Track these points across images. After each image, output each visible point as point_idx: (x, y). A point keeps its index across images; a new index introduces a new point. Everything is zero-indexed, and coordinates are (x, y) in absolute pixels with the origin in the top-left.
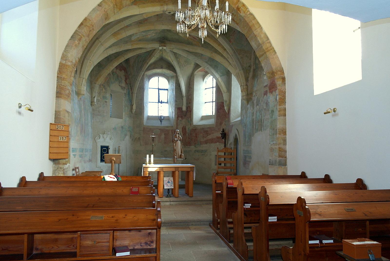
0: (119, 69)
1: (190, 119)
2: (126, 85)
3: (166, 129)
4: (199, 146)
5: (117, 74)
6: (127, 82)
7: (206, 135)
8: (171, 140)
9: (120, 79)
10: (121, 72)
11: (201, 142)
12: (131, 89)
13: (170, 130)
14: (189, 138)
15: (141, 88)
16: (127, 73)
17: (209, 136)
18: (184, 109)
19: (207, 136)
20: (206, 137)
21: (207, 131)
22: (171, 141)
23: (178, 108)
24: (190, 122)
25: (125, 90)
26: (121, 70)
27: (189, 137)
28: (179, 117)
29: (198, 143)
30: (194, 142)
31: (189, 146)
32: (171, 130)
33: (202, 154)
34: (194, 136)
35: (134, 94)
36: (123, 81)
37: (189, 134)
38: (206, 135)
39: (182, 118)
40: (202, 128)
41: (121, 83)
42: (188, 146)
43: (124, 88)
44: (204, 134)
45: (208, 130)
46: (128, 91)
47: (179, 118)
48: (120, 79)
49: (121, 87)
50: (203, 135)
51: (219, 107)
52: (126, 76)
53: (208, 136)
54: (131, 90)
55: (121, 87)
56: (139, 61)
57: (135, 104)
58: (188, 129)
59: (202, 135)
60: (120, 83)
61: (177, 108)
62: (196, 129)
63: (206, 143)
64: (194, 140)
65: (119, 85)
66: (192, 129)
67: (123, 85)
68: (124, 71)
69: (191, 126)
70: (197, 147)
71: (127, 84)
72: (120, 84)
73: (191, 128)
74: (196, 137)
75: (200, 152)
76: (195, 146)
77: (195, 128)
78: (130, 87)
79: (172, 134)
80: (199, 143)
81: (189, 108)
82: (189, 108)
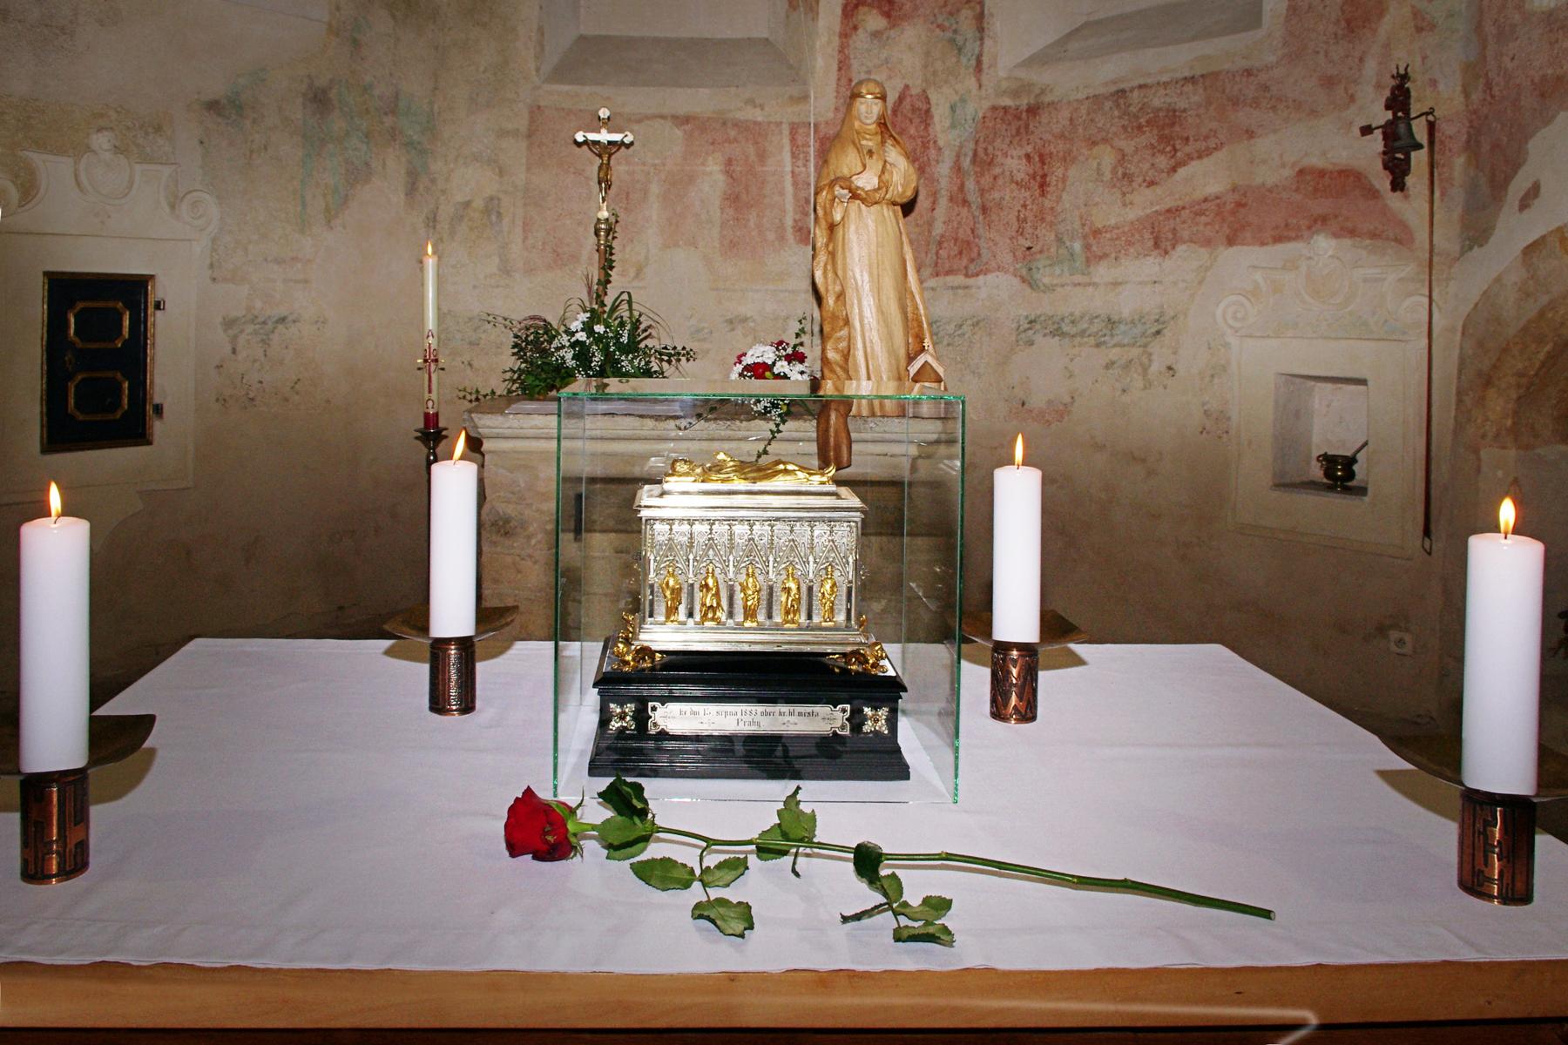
3: (740, 115)
4: (1078, 278)
7: (1162, 161)
8: (789, 222)
11: (1097, 233)
13: (781, 123)
14: (965, 202)
17: (1194, 163)
19: (1174, 169)
20: (1152, 183)
21: (1173, 116)
22: (790, 231)
27: (962, 188)
29: (1059, 240)
30: (1021, 232)
31: (959, 279)
32: (786, 132)
33: (1114, 353)
34: (1019, 176)
37: (957, 168)
40: (1113, 89)
42: (948, 273)
45: (1182, 104)
50: (1122, 157)
53: (1182, 172)
58: (953, 108)
59: (1107, 157)
62: (1033, 110)
63: (1156, 245)
64: (1022, 221)
66: (994, 108)
70: (1050, 289)
73: (986, 104)
75: (1083, 333)
76: (1023, 280)
77: (1024, 102)
79: (793, 164)
80: (1077, 246)
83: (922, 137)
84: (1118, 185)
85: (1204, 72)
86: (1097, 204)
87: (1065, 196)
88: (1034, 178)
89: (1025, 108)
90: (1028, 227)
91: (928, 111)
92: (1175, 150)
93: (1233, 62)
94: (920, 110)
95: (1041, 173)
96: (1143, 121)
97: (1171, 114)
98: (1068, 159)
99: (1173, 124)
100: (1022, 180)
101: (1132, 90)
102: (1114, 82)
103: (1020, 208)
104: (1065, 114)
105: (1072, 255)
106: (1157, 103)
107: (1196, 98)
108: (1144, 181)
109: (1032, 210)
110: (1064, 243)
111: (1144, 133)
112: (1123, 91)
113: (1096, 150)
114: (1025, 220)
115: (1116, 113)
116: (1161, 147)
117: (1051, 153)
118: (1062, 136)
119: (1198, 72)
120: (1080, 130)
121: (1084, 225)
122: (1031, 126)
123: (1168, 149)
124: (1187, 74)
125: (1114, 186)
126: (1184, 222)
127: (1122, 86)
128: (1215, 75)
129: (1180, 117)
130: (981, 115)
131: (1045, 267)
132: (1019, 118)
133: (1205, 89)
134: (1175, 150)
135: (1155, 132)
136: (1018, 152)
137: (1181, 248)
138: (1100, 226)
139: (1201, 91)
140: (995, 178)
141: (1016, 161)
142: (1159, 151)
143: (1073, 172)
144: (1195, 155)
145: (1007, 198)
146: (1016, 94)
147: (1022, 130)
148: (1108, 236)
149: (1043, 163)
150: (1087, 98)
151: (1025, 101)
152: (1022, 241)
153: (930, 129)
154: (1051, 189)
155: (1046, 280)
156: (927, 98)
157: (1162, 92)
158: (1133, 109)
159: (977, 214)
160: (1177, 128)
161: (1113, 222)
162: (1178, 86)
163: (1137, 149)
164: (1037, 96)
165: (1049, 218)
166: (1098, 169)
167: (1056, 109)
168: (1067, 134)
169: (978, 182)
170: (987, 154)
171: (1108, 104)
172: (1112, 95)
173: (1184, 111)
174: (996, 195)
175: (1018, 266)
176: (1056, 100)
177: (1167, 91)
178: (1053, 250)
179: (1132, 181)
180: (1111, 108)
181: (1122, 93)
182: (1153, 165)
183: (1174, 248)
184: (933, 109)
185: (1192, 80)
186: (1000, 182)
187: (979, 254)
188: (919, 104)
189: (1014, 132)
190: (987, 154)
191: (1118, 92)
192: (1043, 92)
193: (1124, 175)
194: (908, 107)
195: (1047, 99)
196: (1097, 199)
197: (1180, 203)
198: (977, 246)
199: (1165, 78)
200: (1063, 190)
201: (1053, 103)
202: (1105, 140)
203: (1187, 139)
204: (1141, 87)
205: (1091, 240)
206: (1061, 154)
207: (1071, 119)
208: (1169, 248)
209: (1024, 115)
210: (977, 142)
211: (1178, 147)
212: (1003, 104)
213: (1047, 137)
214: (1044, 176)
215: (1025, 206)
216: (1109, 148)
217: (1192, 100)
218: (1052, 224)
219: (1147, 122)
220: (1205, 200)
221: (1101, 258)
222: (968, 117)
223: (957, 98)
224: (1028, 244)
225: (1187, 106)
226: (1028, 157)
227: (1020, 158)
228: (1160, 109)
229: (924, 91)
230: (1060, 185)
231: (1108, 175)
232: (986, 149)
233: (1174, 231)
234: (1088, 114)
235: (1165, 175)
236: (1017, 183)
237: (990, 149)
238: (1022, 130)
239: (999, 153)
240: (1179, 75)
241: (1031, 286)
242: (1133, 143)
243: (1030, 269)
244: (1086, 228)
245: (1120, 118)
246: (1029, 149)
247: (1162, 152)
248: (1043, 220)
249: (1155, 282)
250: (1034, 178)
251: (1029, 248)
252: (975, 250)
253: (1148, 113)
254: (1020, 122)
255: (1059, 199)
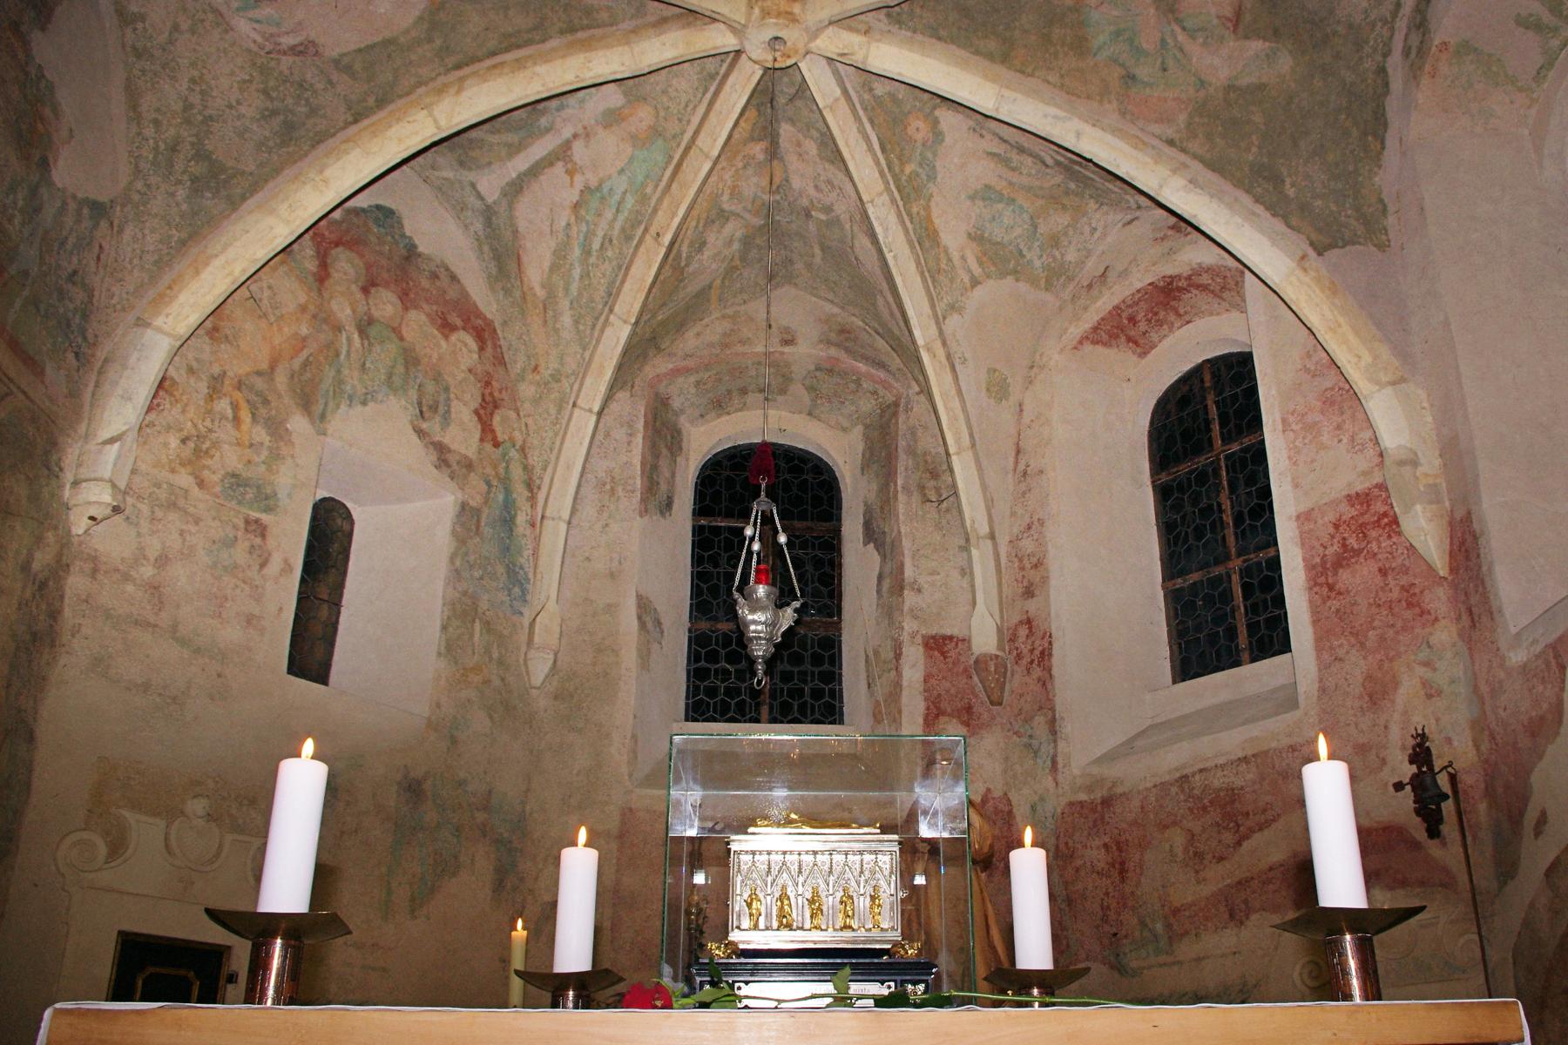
0: (428, 315)
1: (1040, 721)
2: (488, 446)
5: (402, 339)
6: (498, 429)
7: (1228, 837)
9: (430, 387)
10: (446, 337)
11: (1176, 912)
12: (530, 486)
15: (613, 490)
16: (500, 361)
18: (984, 637)
19: (1239, 843)
20: (1221, 859)
23: (933, 637)
24: (1047, 749)
25: (474, 479)
26: (446, 328)
28: (940, 713)
29: (1143, 924)
34: (1101, 865)
35: (548, 524)
36: (464, 412)
38: (1228, 837)
39: (967, 724)
40: (1178, 775)
41: (438, 419)
43: (469, 466)
44: (1197, 829)
45: (1239, 782)
46: (501, 497)
47: (943, 719)
48: (430, 387)
49: (441, 449)
51: (1335, 548)
52: (488, 384)
54: (532, 499)
55: (441, 449)
56: (596, 245)
57: (552, 605)
59: (1178, 839)
60: (421, 412)
61: (923, 636)
62: (1107, 802)
64: (1105, 909)
65: (420, 433)
66: (1071, 804)
67: (463, 436)
68: (473, 344)
69: (1055, 780)
71: (497, 445)
72: (424, 426)
73: (1064, 801)
74: (1123, 872)
76: (1112, 967)
77: (1098, 795)
78: (517, 473)
80: (1159, 927)
81: (1031, 633)
82: (1031, 633)
83: (1006, 837)
84: (1191, 864)
85: (1256, 751)
86: (1174, 883)
87: (1143, 880)
88: (1114, 867)
89: (1099, 801)
90: (1112, 915)
91: (1010, 812)
92: (1238, 826)
93: (1278, 741)
94: (1002, 811)
95: (1119, 860)
96: (1206, 801)
97: (1230, 792)
98: (1143, 845)
99: (1233, 802)
100: (1103, 869)
101: (1194, 774)
102: (1177, 770)
103: (1102, 896)
104: (1136, 803)
105: (1155, 936)
106: (1217, 783)
107: (1250, 776)
108: (1214, 857)
109: (1113, 897)
110: (1146, 925)
111: (1209, 812)
112: (1186, 776)
113: (1167, 833)
114: (1108, 908)
115: (1182, 797)
116: (1225, 825)
117: (1127, 840)
118: (1135, 823)
119: (1250, 752)
120: (1152, 816)
121: (1163, 906)
122: (1107, 816)
123: (1231, 825)
124: (1241, 755)
125: (1187, 865)
126: (1254, 892)
127: (1185, 772)
128: (1266, 753)
129: (1238, 795)
130: (1059, 811)
131: (1131, 951)
132: (1094, 810)
133: (1257, 767)
134: (1238, 826)
135: (1218, 810)
136: (1097, 842)
137: (1254, 917)
138: (1179, 905)
139: (1254, 769)
140: (1077, 870)
141: (1095, 852)
142: (1224, 828)
143: (1149, 856)
144: (1257, 828)
145: (1090, 887)
146: (1089, 789)
147: (1099, 822)
148: (1187, 913)
149: (1121, 851)
150: (1155, 786)
151: (1100, 795)
152: (1107, 928)
153: (1014, 829)
154: (1129, 875)
155: (1134, 964)
156: (1009, 800)
157: (1220, 774)
158: (1196, 792)
159: (1063, 906)
160: (1237, 805)
161: (1190, 899)
162: (1234, 766)
163: (1204, 830)
164: (1110, 788)
165: (1130, 903)
166: (1171, 851)
167: (1128, 799)
168: (1140, 821)
169: (1061, 876)
170: (1068, 849)
171: (1174, 790)
172: (1177, 781)
173: (1242, 788)
174: (1080, 886)
175: (1106, 953)
176: (1127, 791)
177: (1225, 773)
178: (1137, 933)
179: (1204, 858)
180: (1177, 793)
181: (1185, 778)
182: (1220, 842)
183: (1247, 918)
184: (1014, 810)
185: (1245, 760)
186: (1083, 873)
187: (1068, 946)
188: (1001, 806)
189: (1091, 824)
190: (1068, 849)
191: (1181, 777)
192: (1114, 785)
193: (1196, 854)
194: (991, 809)
195: (1119, 790)
196: (1173, 880)
197: (1248, 874)
198: (1066, 937)
199: (1221, 761)
200: (1141, 874)
201: (1124, 793)
202: (1175, 823)
203: (1248, 814)
204: (1201, 771)
205: (1172, 920)
206: (1136, 841)
207: (1142, 808)
208: (1244, 918)
209: (1099, 808)
210: (1058, 838)
211: (1240, 822)
212: (1079, 799)
213: (1124, 826)
214: (1122, 863)
215: (1107, 894)
216: (1179, 831)
217: (1247, 778)
218: (1133, 909)
219: (1211, 802)
220: (1271, 869)
221: (1183, 935)
222: (1048, 814)
223: (1037, 798)
224: (1114, 930)
225: (1243, 784)
226: (1106, 846)
227: (1098, 848)
228: (1221, 789)
229: (1005, 794)
230: (1138, 870)
231: (1180, 856)
232: (1067, 843)
233: (1246, 902)
234: (1157, 800)
235: (1232, 849)
236: (1098, 873)
237: (1071, 844)
238: (1099, 822)
239: (1080, 846)
240: (1233, 757)
241: (1122, 974)
242: (1199, 823)
243: (1118, 955)
244: (1166, 908)
245: (1186, 801)
246: (1107, 839)
247: (1226, 828)
248: (1125, 905)
249: (1235, 953)
250: (1114, 867)
251: (1115, 935)
252: (1064, 942)
253: (1210, 794)
254: (1097, 815)
255: (1138, 884)
